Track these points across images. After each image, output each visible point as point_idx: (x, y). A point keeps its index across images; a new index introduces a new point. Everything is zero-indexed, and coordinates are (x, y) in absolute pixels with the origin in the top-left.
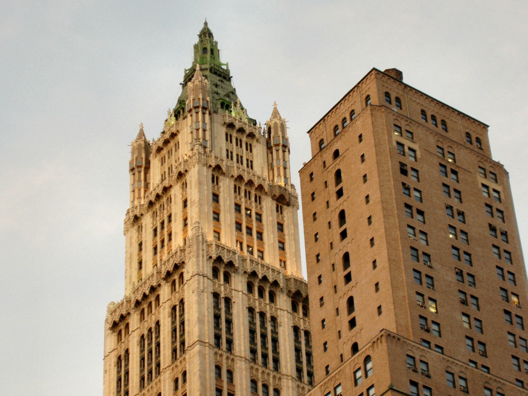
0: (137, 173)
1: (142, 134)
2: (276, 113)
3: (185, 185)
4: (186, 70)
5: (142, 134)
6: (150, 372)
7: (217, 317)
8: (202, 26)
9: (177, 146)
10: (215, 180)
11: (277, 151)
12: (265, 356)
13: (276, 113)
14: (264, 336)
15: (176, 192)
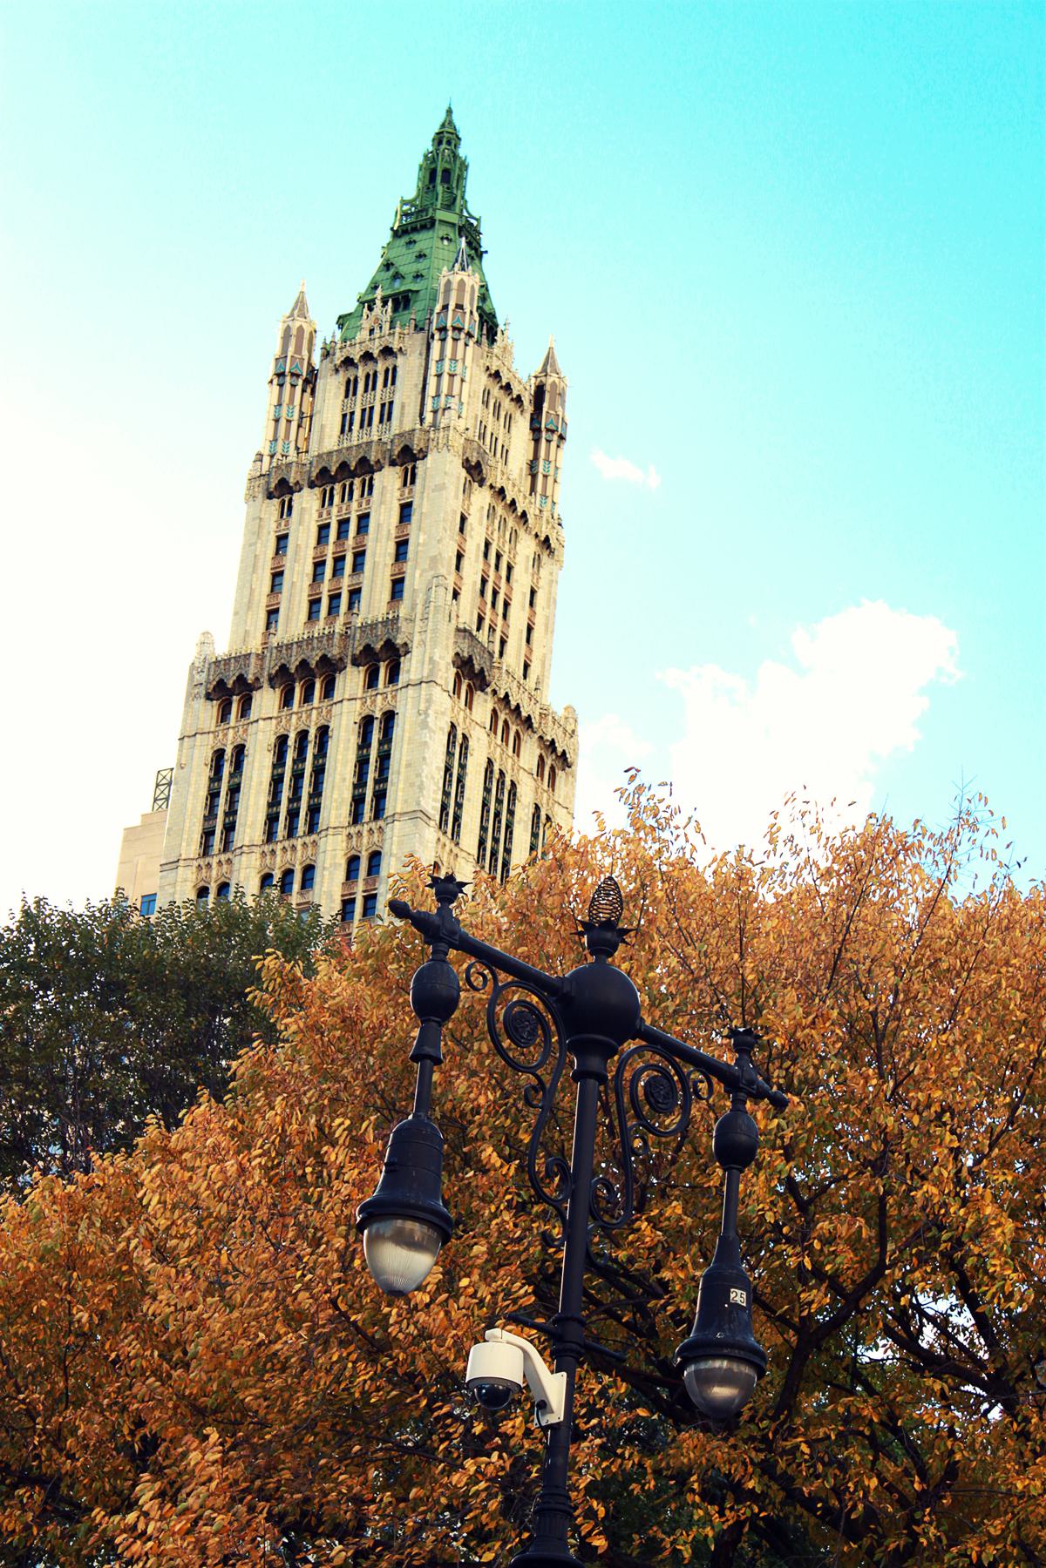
0: (287, 387)
1: (300, 307)
2: (549, 361)
3: (410, 478)
4: (404, 203)
5: (300, 307)
6: (293, 814)
7: (448, 769)
8: (442, 117)
9: (391, 375)
10: (467, 490)
11: (549, 441)
12: (494, 854)
13: (549, 361)
14: (497, 814)
15: (388, 480)
